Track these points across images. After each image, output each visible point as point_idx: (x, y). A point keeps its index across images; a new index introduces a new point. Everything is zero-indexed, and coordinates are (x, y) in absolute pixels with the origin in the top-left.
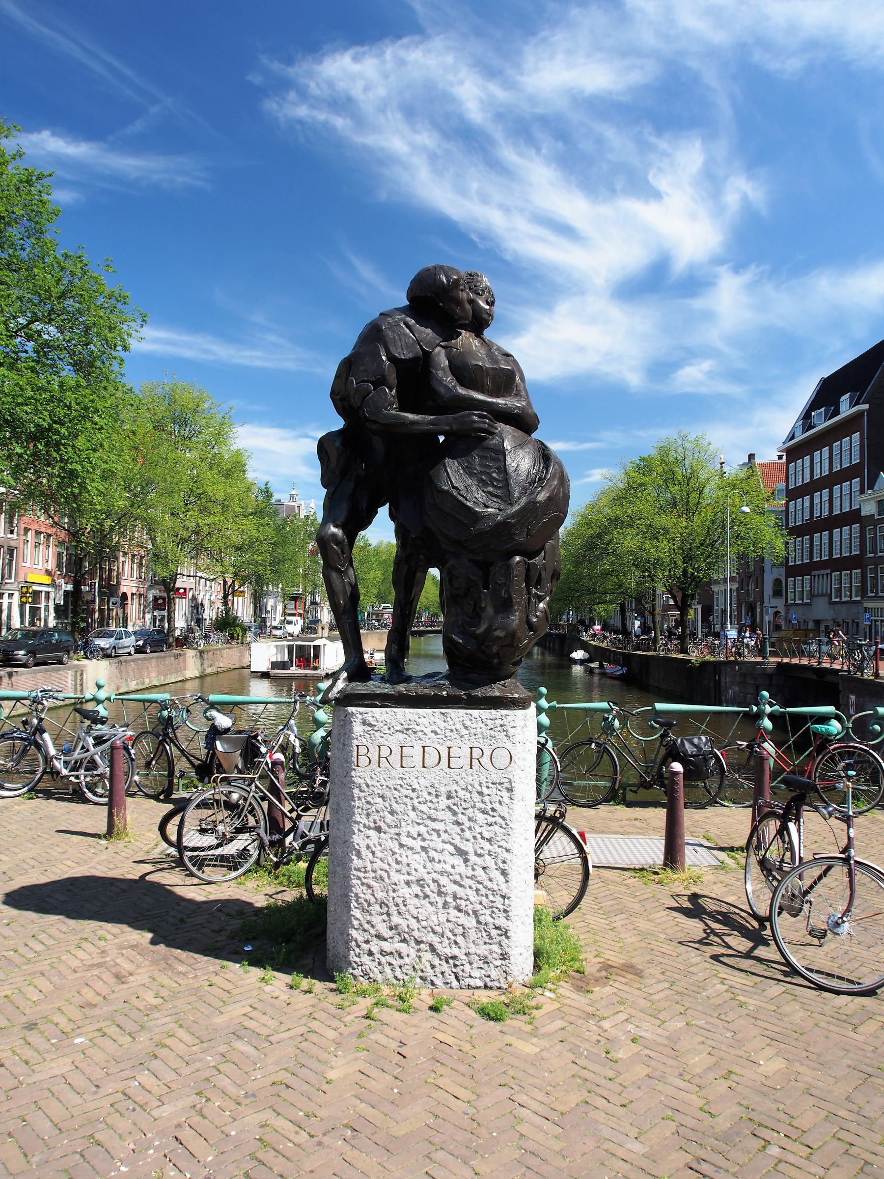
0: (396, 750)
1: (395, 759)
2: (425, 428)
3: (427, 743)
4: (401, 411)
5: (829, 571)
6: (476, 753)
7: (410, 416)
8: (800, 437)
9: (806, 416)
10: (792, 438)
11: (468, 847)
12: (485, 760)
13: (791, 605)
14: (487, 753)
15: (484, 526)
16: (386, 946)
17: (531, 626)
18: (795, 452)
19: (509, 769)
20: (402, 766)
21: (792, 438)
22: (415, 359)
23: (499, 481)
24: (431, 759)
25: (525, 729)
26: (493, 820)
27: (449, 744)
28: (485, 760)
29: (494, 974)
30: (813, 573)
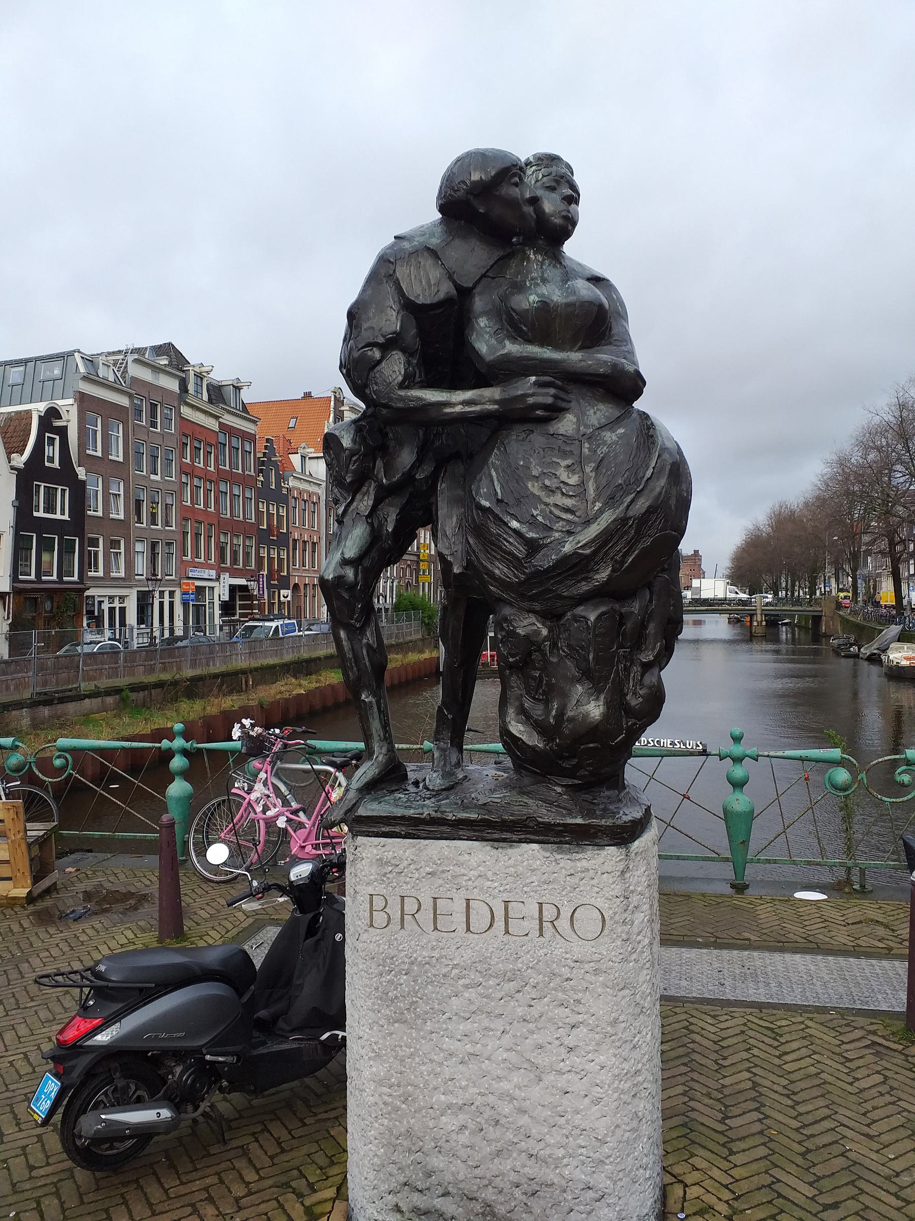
0: (427, 904)
1: (426, 916)
2: (458, 409)
3: (475, 894)
6: (549, 913)
12: (563, 924)
14: (566, 913)
19: (601, 939)
20: (436, 928)
22: (447, 302)
24: (480, 919)
25: (627, 875)
26: (580, 1018)
27: (506, 896)
28: (563, 924)
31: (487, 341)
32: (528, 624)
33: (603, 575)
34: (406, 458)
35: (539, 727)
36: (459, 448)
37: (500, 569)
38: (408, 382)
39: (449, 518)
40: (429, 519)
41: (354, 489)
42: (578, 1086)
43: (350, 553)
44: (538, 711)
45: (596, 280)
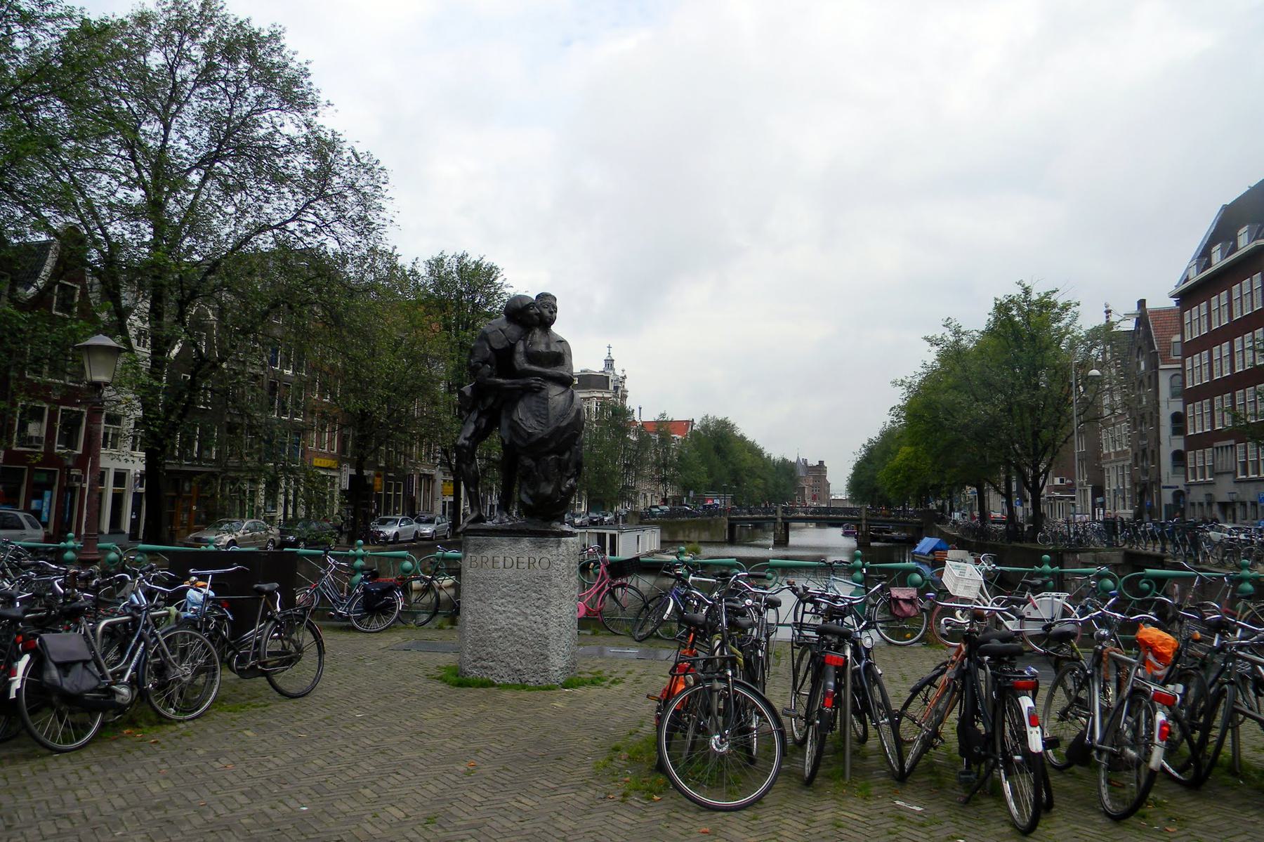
1: (490, 563)
4: (499, 376)
5: (1232, 442)
7: (501, 380)
8: (1195, 277)
9: (1204, 255)
10: (1187, 280)
11: (528, 611)
13: (1192, 484)
15: (533, 439)
16: (485, 663)
17: (562, 493)
18: (1189, 296)
21: (1187, 280)
23: (542, 414)
24: (508, 563)
28: (537, 564)
29: (541, 680)
30: (1216, 444)
31: (520, 361)
32: (528, 462)
33: (552, 445)
34: (490, 401)
35: (531, 497)
36: (509, 399)
37: (519, 442)
38: (490, 375)
39: (505, 423)
40: (498, 424)
41: (470, 412)
42: (539, 620)
43: (468, 435)
44: (531, 492)
45: (561, 341)
